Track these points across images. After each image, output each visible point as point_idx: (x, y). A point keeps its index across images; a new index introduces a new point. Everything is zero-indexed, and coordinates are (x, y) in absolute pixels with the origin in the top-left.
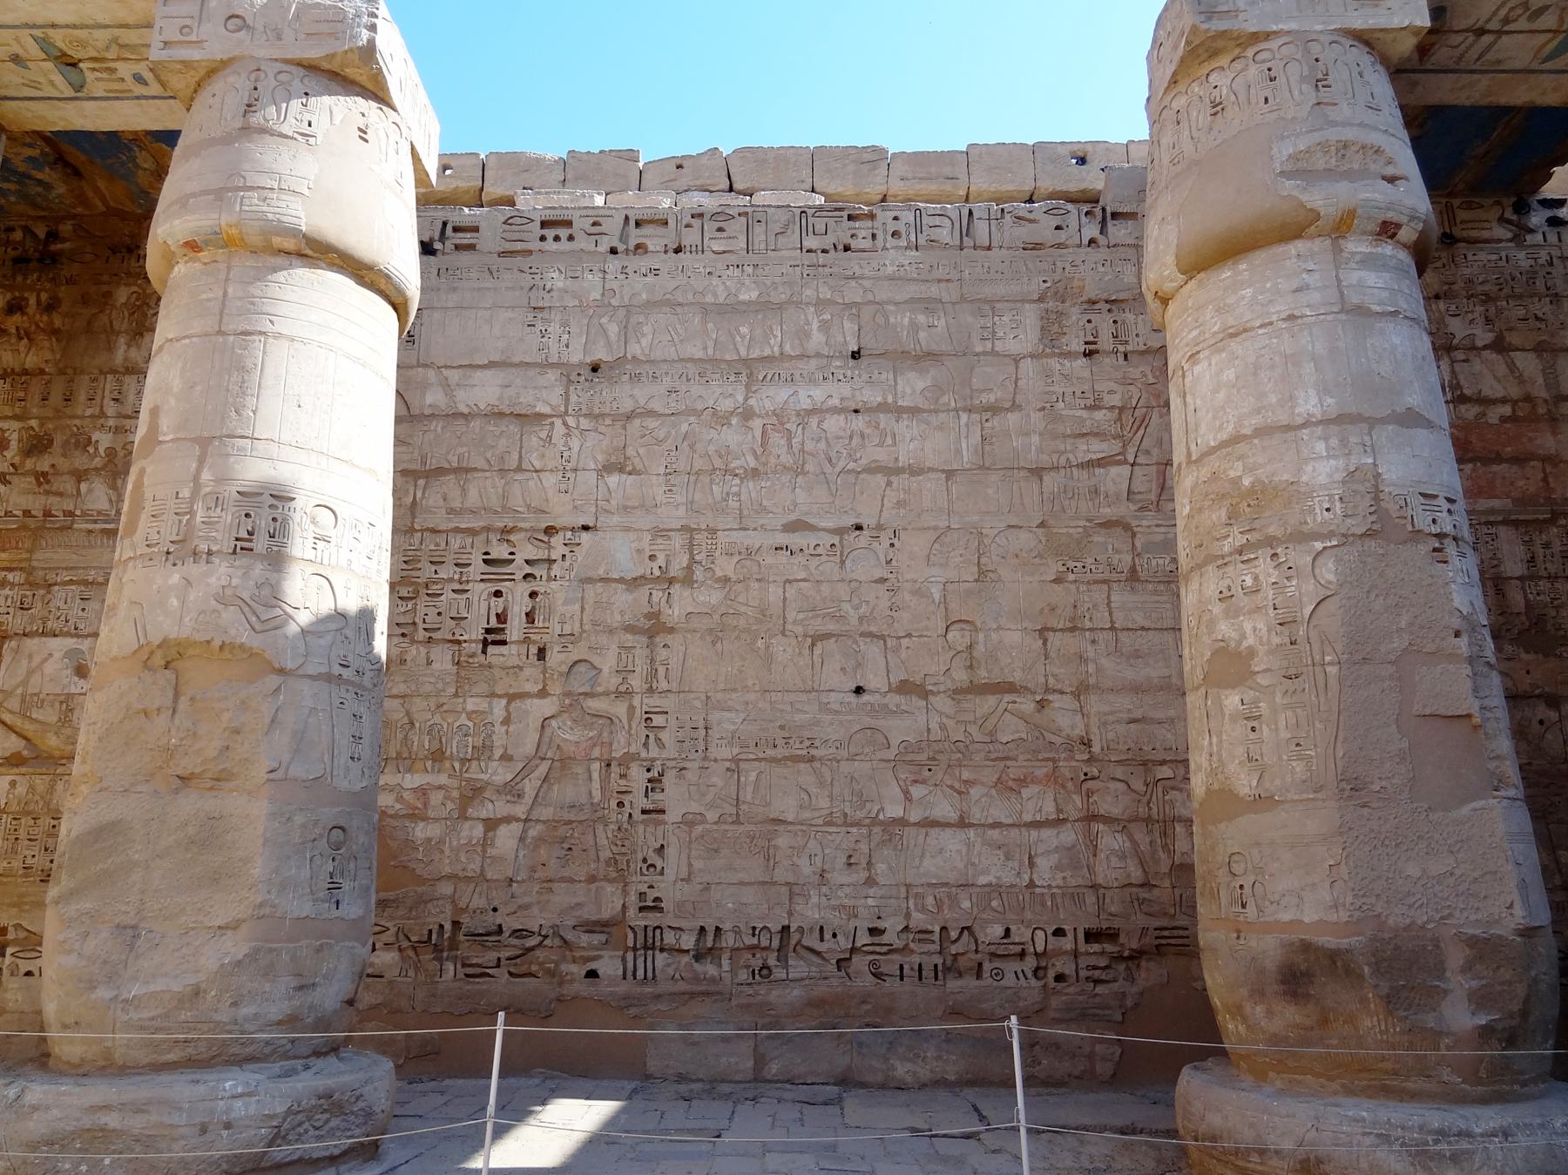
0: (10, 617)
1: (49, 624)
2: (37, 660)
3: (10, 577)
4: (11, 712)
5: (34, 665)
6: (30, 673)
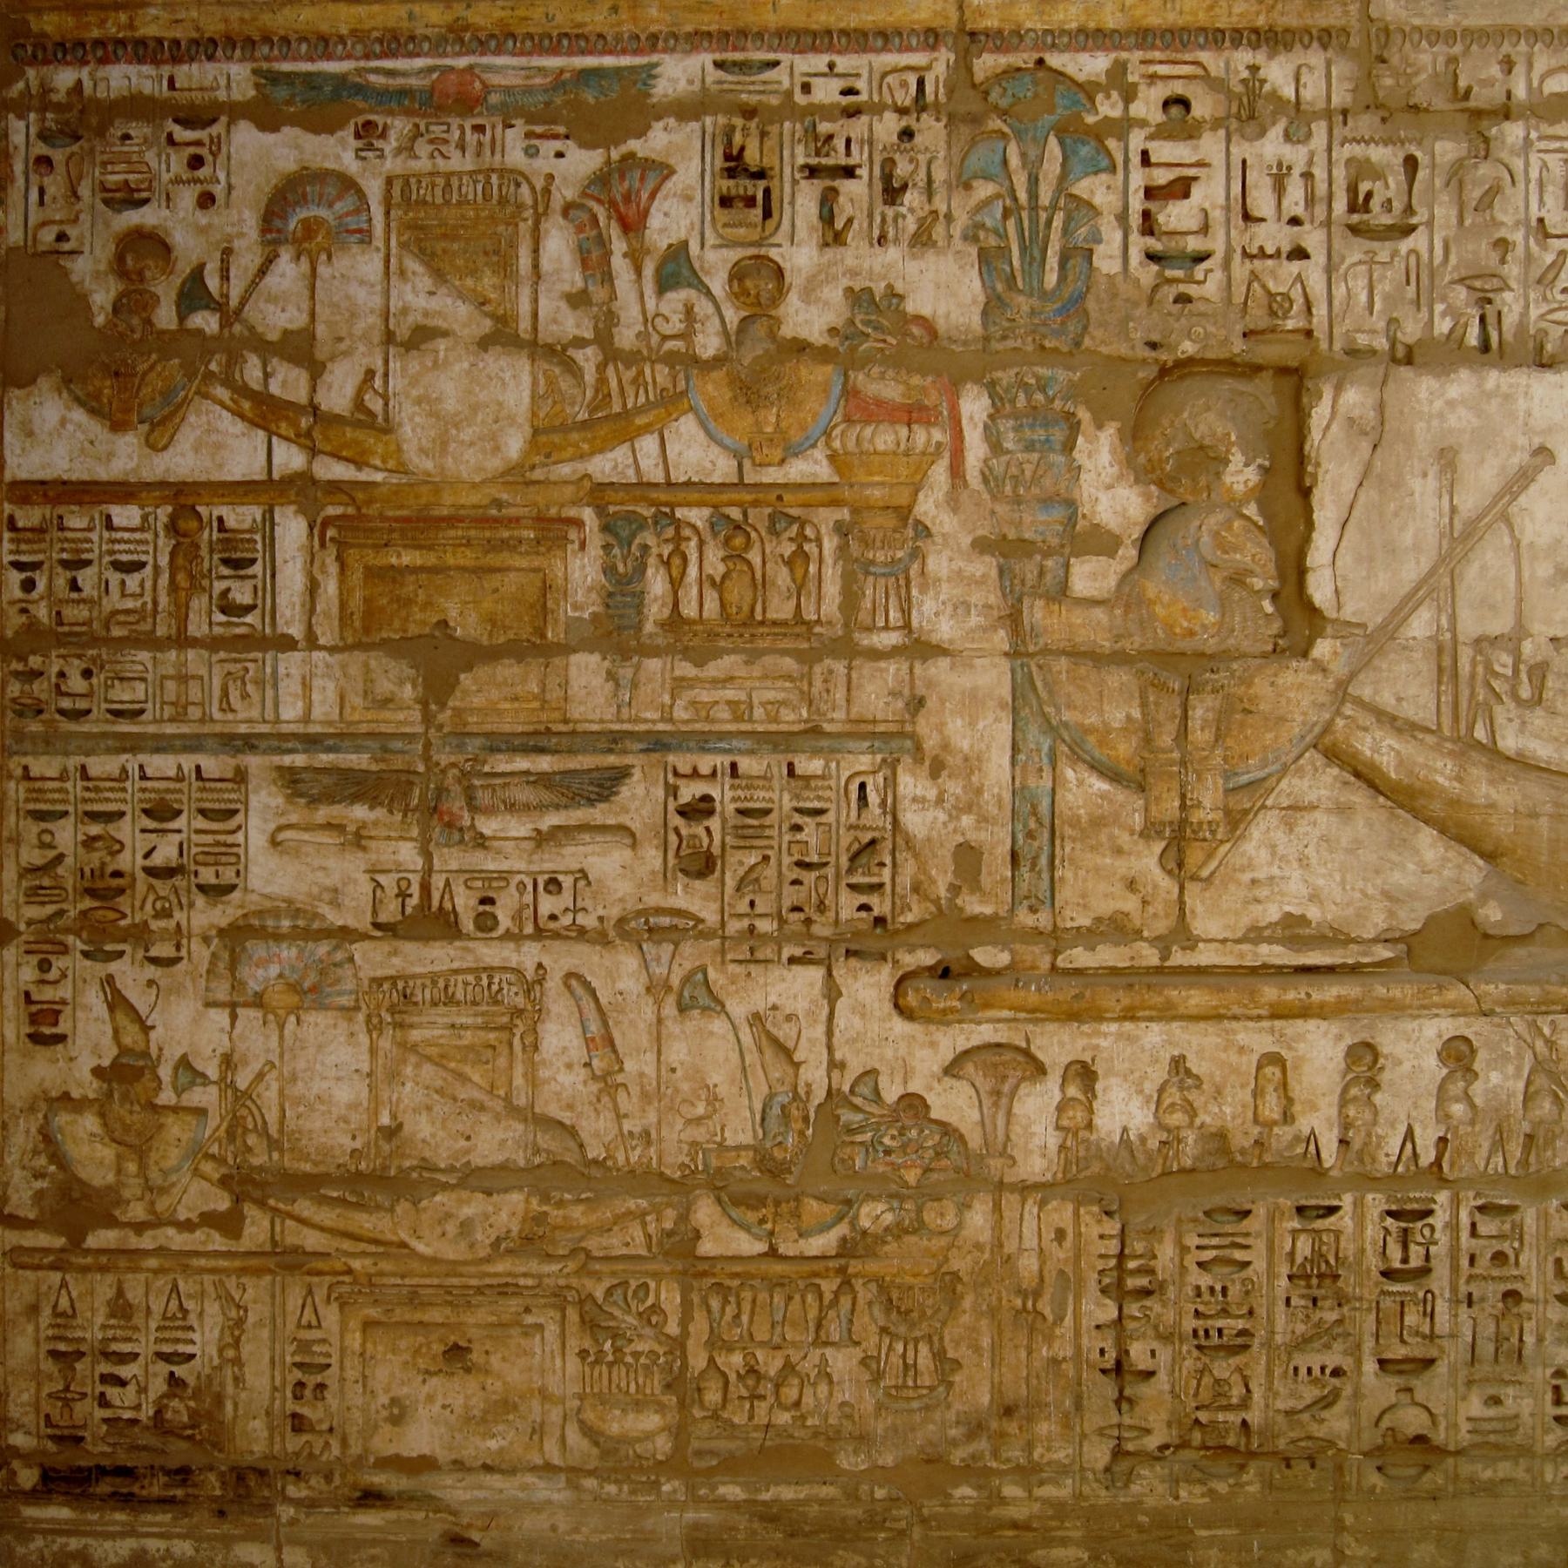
0: (1314, 272)
1: (1510, 304)
2: (1481, 479)
3: (1278, 73)
4: (1407, 728)
5: (1468, 502)
6: (1461, 539)
